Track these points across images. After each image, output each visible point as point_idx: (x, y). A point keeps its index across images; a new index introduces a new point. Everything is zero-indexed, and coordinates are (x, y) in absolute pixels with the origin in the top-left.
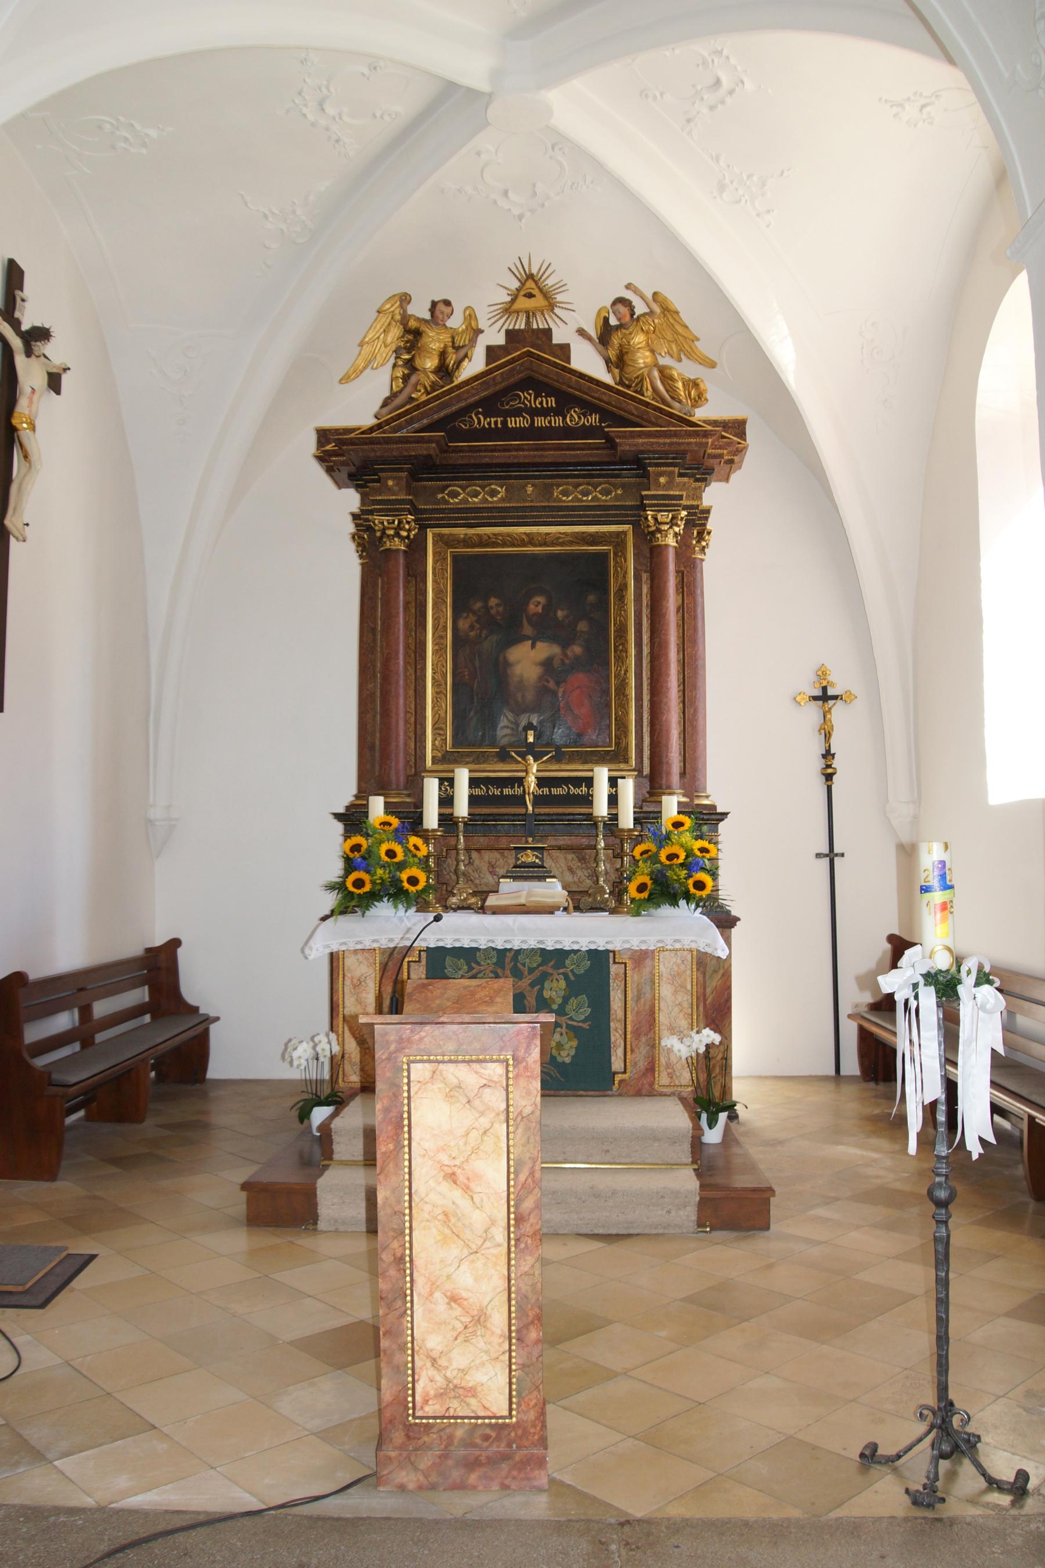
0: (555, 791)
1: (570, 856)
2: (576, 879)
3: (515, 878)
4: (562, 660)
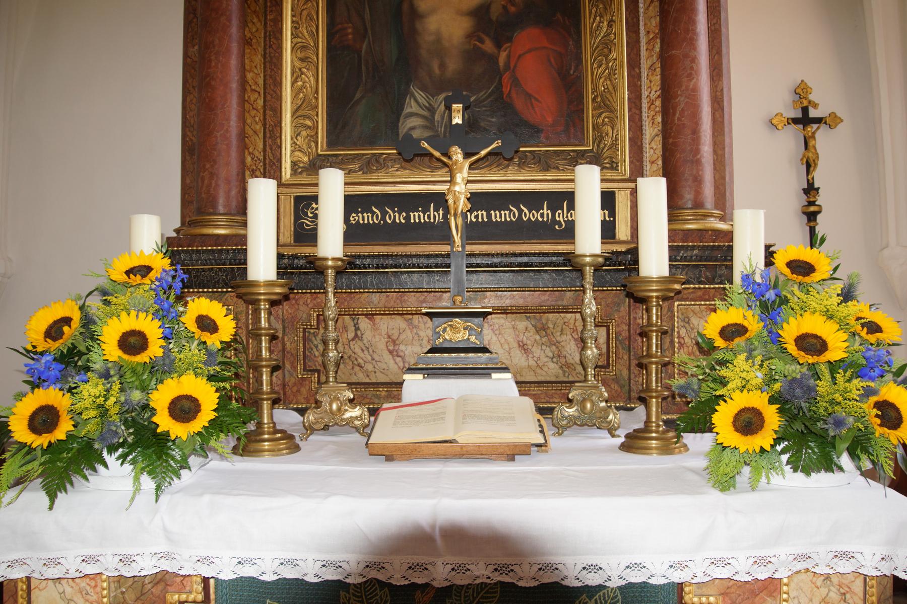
0: (496, 216)
1: (522, 324)
2: (532, 363)
3: (432, 372)
4: (504, 7)
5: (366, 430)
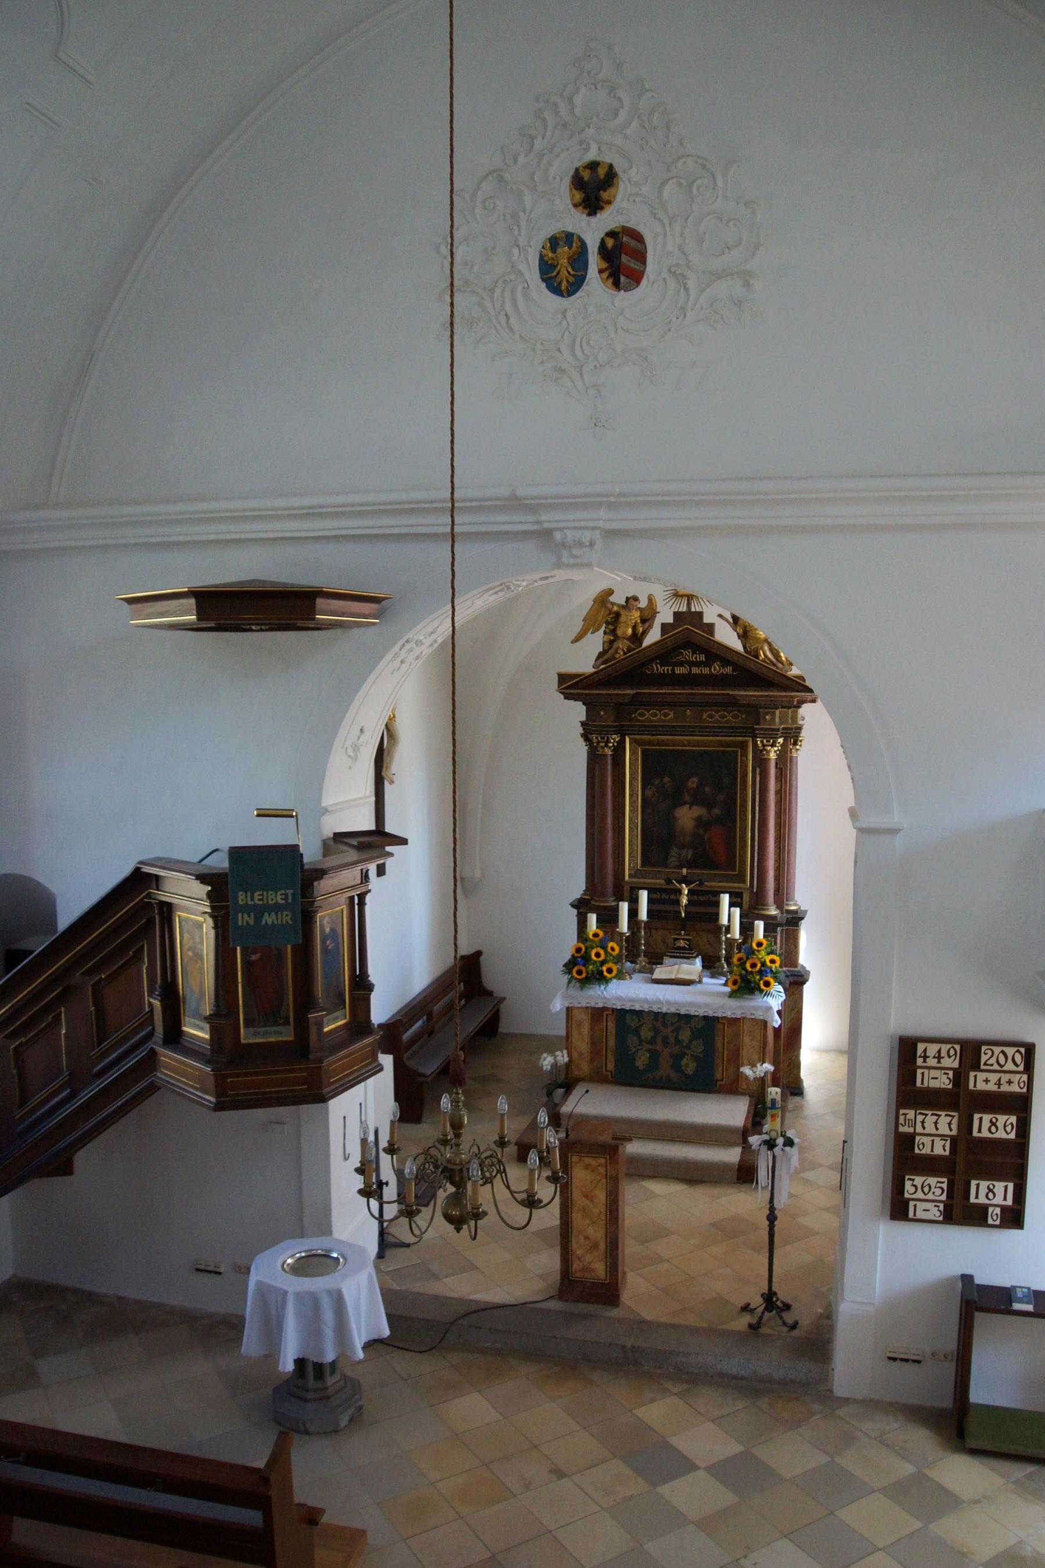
0: (701, 898)
1: (710, 936)
3: (672, 957)
5: (651, 972)
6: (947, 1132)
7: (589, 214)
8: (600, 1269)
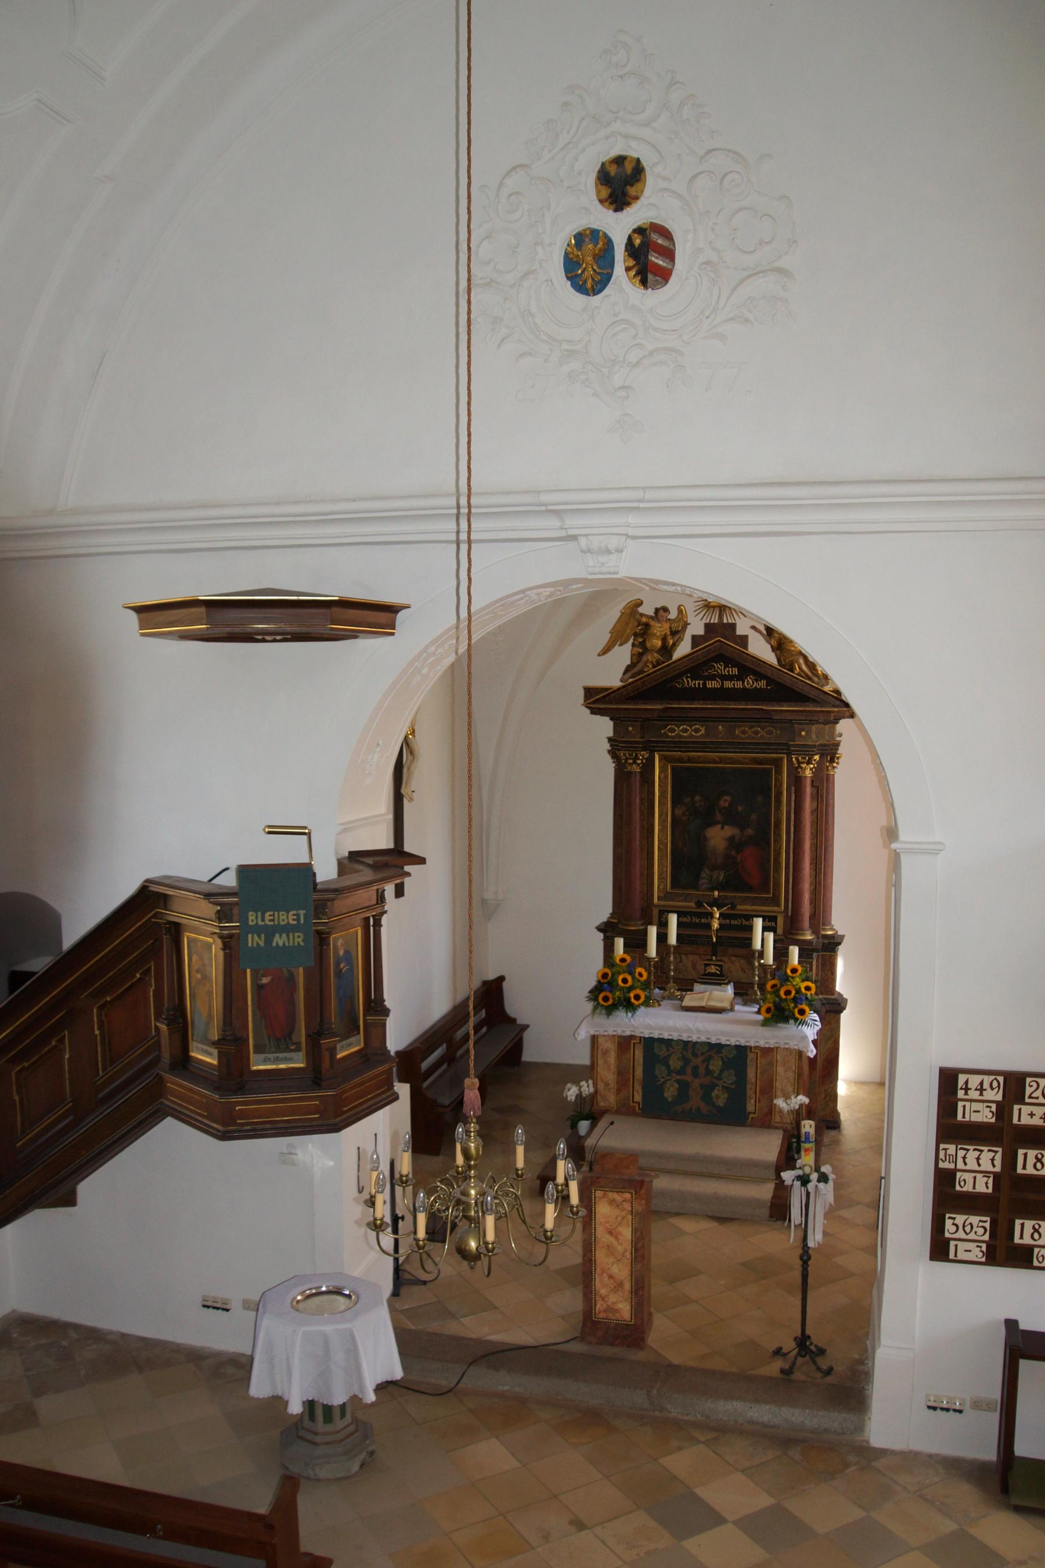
0: (733, 922)
1: (742, 961)
3: (702, 983)
5: (682, 999)
6: (990, 1169)
7: (616, 210)
8: (624, 1310)
